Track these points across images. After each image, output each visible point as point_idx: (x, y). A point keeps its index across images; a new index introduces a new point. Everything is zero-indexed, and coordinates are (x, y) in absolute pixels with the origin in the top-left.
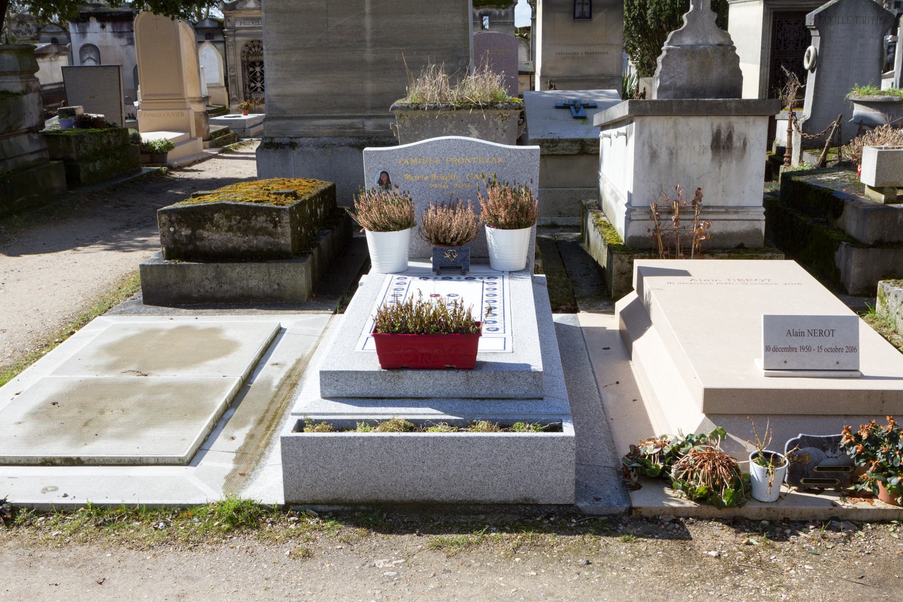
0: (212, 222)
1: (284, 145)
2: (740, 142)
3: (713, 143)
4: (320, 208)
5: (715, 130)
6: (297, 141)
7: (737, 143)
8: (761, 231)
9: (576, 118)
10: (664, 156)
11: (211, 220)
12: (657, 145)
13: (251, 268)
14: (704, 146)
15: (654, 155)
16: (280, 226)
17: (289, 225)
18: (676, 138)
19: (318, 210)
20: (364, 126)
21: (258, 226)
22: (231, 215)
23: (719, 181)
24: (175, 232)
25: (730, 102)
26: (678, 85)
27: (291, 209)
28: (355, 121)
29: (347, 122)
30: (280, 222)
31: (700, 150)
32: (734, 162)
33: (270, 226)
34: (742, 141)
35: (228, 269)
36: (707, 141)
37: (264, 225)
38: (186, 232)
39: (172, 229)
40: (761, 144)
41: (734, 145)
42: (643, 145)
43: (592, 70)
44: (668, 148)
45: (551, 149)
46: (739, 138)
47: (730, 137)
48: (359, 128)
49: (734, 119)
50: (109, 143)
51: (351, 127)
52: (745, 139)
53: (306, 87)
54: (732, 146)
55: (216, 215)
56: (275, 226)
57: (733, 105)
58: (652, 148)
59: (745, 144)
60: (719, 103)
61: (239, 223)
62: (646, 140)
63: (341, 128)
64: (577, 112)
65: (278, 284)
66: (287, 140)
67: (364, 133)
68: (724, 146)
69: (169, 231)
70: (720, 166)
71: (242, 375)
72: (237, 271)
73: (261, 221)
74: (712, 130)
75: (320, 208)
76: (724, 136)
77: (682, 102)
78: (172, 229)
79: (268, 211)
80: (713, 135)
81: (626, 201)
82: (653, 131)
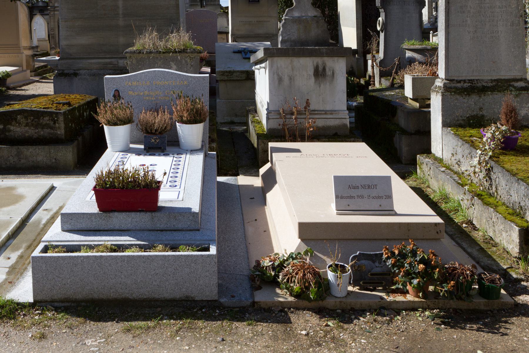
0: (16, 121)
1: (71, 74)
2: (330, 72)
3: (314, 72)
4: (86, 112)
5: (315, 65)
6: (78, 72)
7: (329, 73)
9: (245, 58)
12: (282, 74)
14: (309, 74)
15: (280, 80)
16: (58, 123)
17: (63, 122)
18: (293, 69)
19: (85, 113)
20: (118, 63)
21: (44, 123)
23: (320, 95)
25: (322, 49)
26: (292, 39)
27: (65, 113)
28: (113, 60)
30: (57, 120)
31: (307, 76)
32: (328, 83)
33: (52, 123)
34: (331, 72)
36: (311, 72)
37: (48, 122)
40: (343, 73)
41: (327, 74)
42: (274, 74)
43: (261, 31)
44: (289, 76)
45: (229, 77)
46: (330, 70)
47: (324, 69)
48: (116, 64)
49: (326, 59)
51: (110, 63)
53: (84, 40)
54: (326, 74)
55: (19, 116)
56: (55, 123)
57: (324, 50)
58: (279, 76)
59: (333, 74)
60: (316, 49)
61: (33, 121)
62: (275, 71)
63: (104, 64)
64: (246, 55)
66: (72, 72)
67: (118, 67)
68: (321, 74)
70: (320, 86)
72: (30, 151)
73: (46, 120)
74: (314, 65)
75: (86, 112)
76: (321, 69)
77: (294, 49)
79: (51, 113)
80: (314, 68)
81: (266, 107)
82: (279, 66)
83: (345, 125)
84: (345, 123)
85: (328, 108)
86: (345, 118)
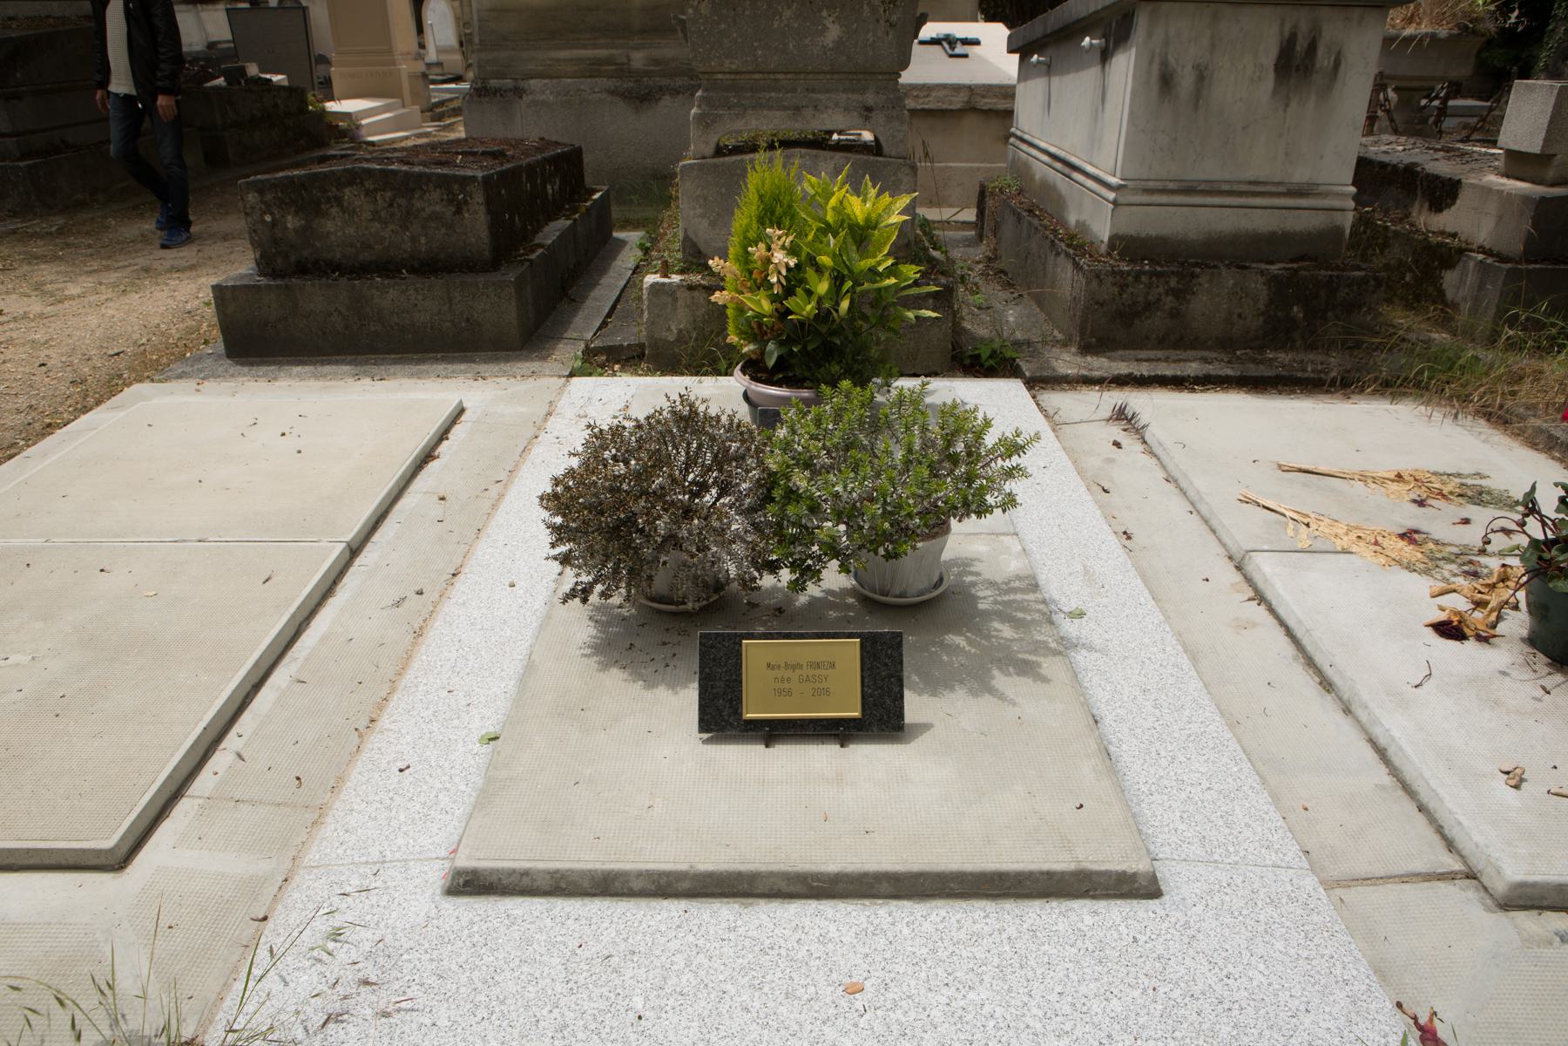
0: (340, 205)
1: (506, 91)
2: (1329, 58)
5: (1287, 34)
6: (522, 84)
7: (1323, 59)
8: (1344, 231)
9: (951, 56)
10: (1186, 81)
11: (339, 201)
12: (1176, 60)
13: (416, 290)
14: (1262, 65)
15: (1166, 81)
16: (468, 210)
17: (483, 208)
18: (1213, 46)
19: (549, 187)
20: (629, 60)
21: (428, 210)
22: (376, 190)
24: (274, 224)
27: (487, 180)
28: (614, 51)
29: (602, 53)
31: (1254, 73)
32: (1313, 97)
33: (449, 212)
34: (1333, 58)
35: (374, 291)
36: (1269, 53)
37: (438, 208)
38: (292, 222)
39: (268, 218)
40: (1368, 64)
41: (1318, 65)
42: (1151, 63)
45: (921, 101)
47: (1312, 48)
48: (623, 64)
49: (1324, 12)
50: (276, 106)
51: (609, 61)
52: (1339, 53)
54: (1313, 65)
55: (347, 191)
56: (459, 211)
58: (1166, 66)
61: (391, 205)
62: (1158, 51)
63: (593, 64)
64: (953, 48)
65: (468, 320)
66: (508, 83)
67: (629, 72)
68: (1298, 66)
69: (263, 221)
70: (1287, 105)
71: (348, 538)
73: (432, 202)
74: (1282, 33)
78: (268, 218)
79: (445, 182)
80: (1281, 43)
83: (1337, 231)
84: (1338, 223)
85: (1300, 176)
86: (1343, 210)
